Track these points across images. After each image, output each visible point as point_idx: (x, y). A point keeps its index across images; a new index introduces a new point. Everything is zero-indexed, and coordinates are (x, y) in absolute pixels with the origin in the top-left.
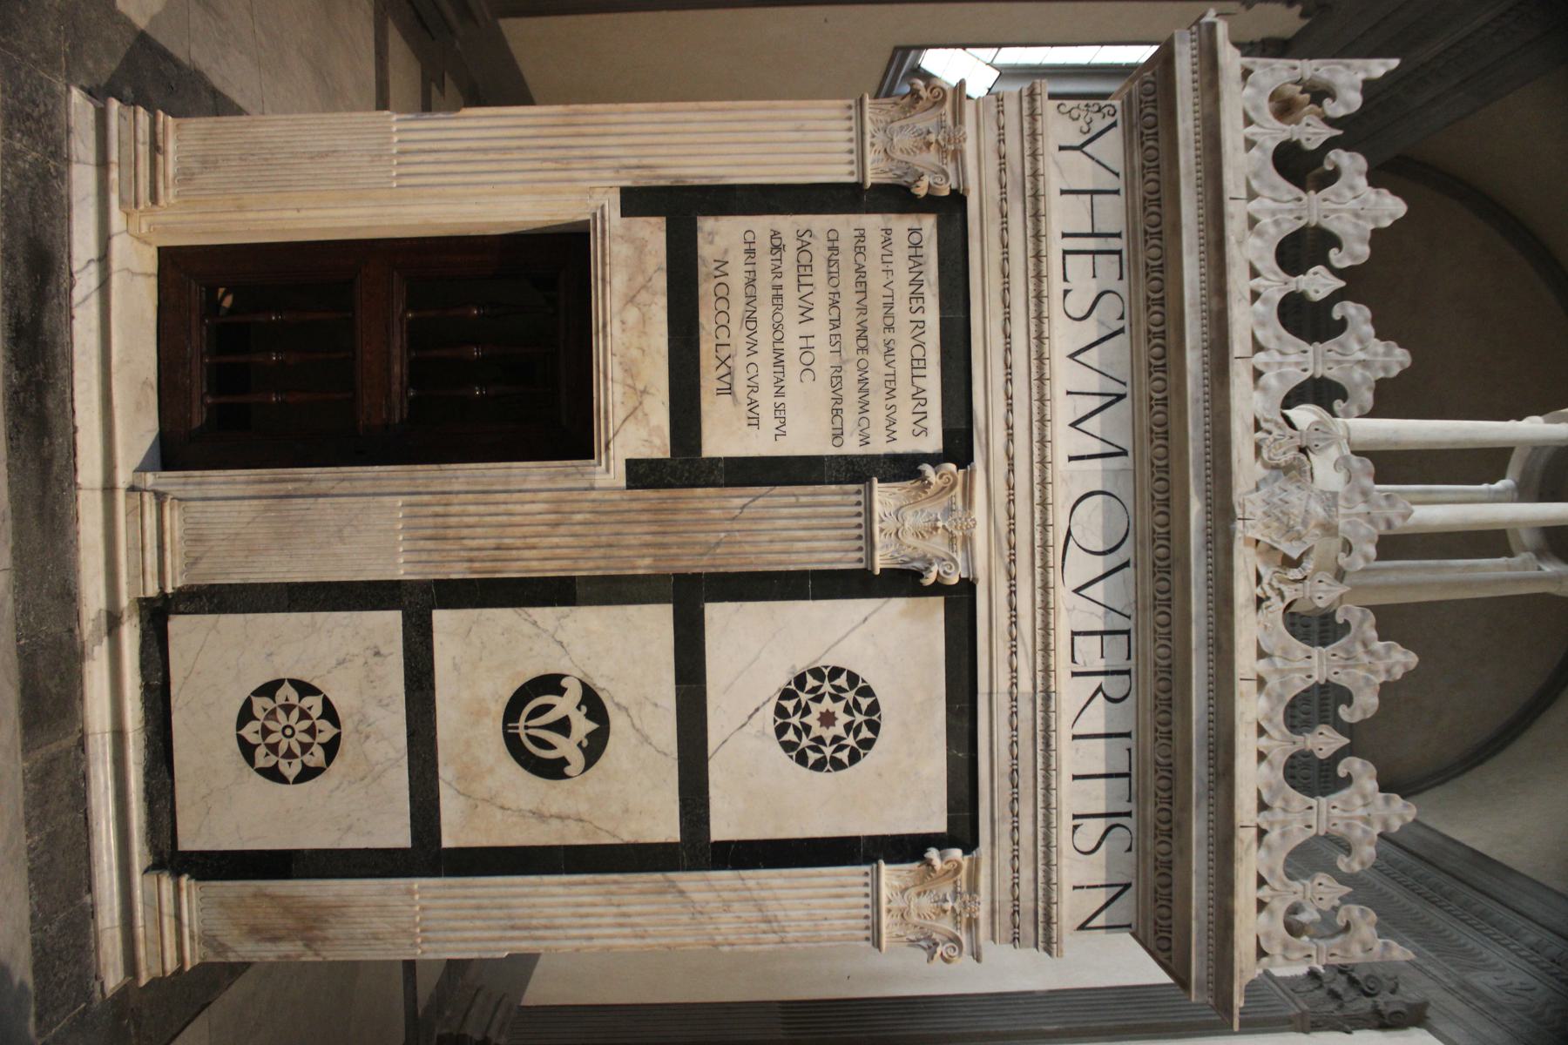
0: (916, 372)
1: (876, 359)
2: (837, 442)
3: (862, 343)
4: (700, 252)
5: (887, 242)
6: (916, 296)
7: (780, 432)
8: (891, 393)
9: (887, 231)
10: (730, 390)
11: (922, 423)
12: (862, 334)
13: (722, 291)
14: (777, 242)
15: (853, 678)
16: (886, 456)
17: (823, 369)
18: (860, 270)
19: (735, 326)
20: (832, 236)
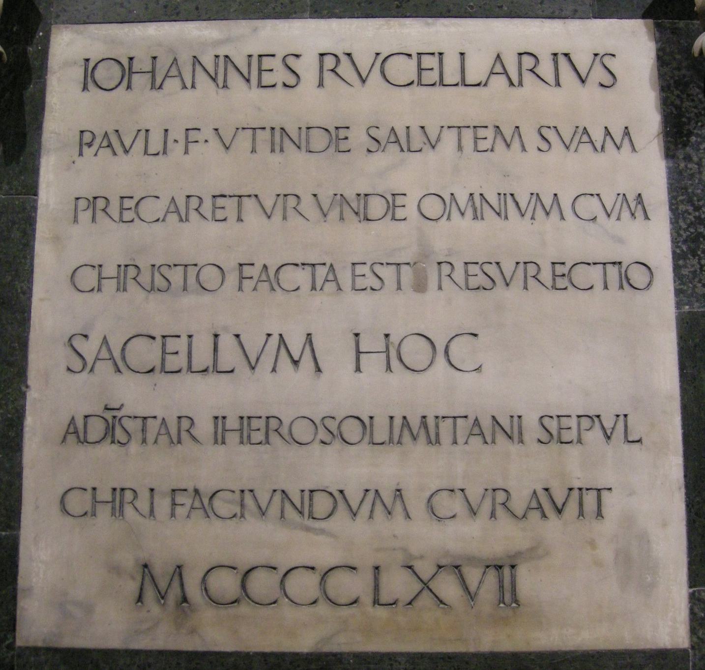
0: (452, 75)
1: (410, 175)
2: (638, 276)
3: (377, 207)
4: (115, 643)
5: (111, 142)
6: (255, 70)
7: (618, 429)
8: (507, 137)
9: (85, 141)
10: (503, 567)
11: (583, 62)
12: (356, 207)
13: (225, 584)
14: (96, 429)
16: (669, 154)
17: (441, 310)
18: (183, 209)
19: (325, 554)
20: (88, 278)
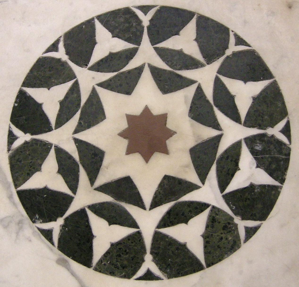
15: (45, 72)
